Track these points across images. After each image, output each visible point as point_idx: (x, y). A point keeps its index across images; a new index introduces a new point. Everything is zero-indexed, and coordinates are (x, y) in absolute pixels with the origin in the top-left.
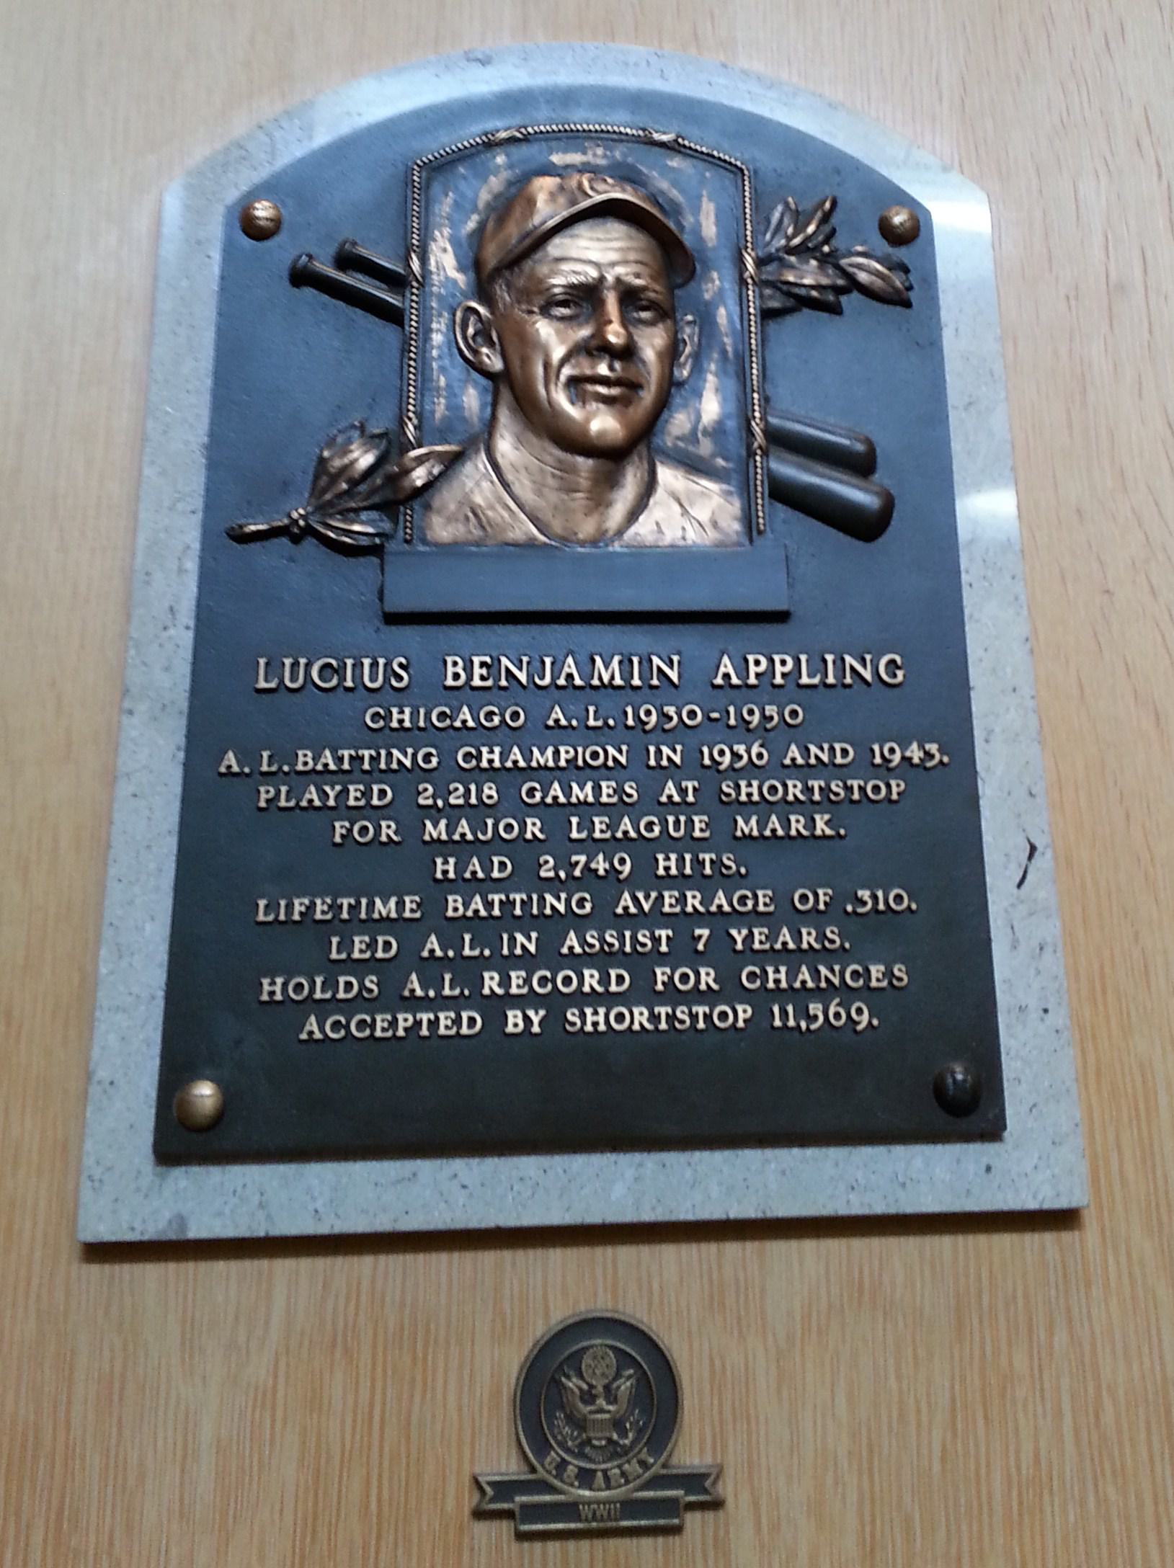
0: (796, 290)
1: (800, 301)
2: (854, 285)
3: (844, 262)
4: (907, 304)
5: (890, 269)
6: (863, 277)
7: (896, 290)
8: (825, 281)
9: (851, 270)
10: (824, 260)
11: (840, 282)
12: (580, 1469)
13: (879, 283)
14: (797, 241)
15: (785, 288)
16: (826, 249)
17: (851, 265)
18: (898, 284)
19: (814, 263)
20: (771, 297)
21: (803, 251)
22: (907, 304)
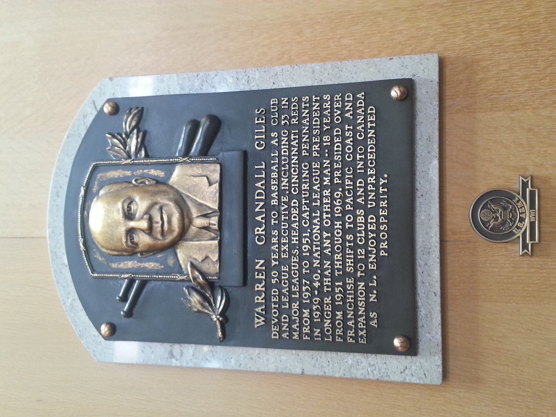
0: (139, 146)
1: (142, 145)
2: (137, 126)
3: (128, 130)
4: (143, 108)
5: (131, 114)
6: (134, 123)
7: (138, 112)
8: (135, 136)
9: (131, 127)
10: (128, 136)
11: (135, 131)
12: (519, 221)
13: (136, 118)
14: (121, 146)
15: (138, 150)
16: (124, 136)
17: (130, 127)
18: (136, 111)
19: (128, 141)
20: (141, 155)
21: (125, 144)
22: (143, 108)
